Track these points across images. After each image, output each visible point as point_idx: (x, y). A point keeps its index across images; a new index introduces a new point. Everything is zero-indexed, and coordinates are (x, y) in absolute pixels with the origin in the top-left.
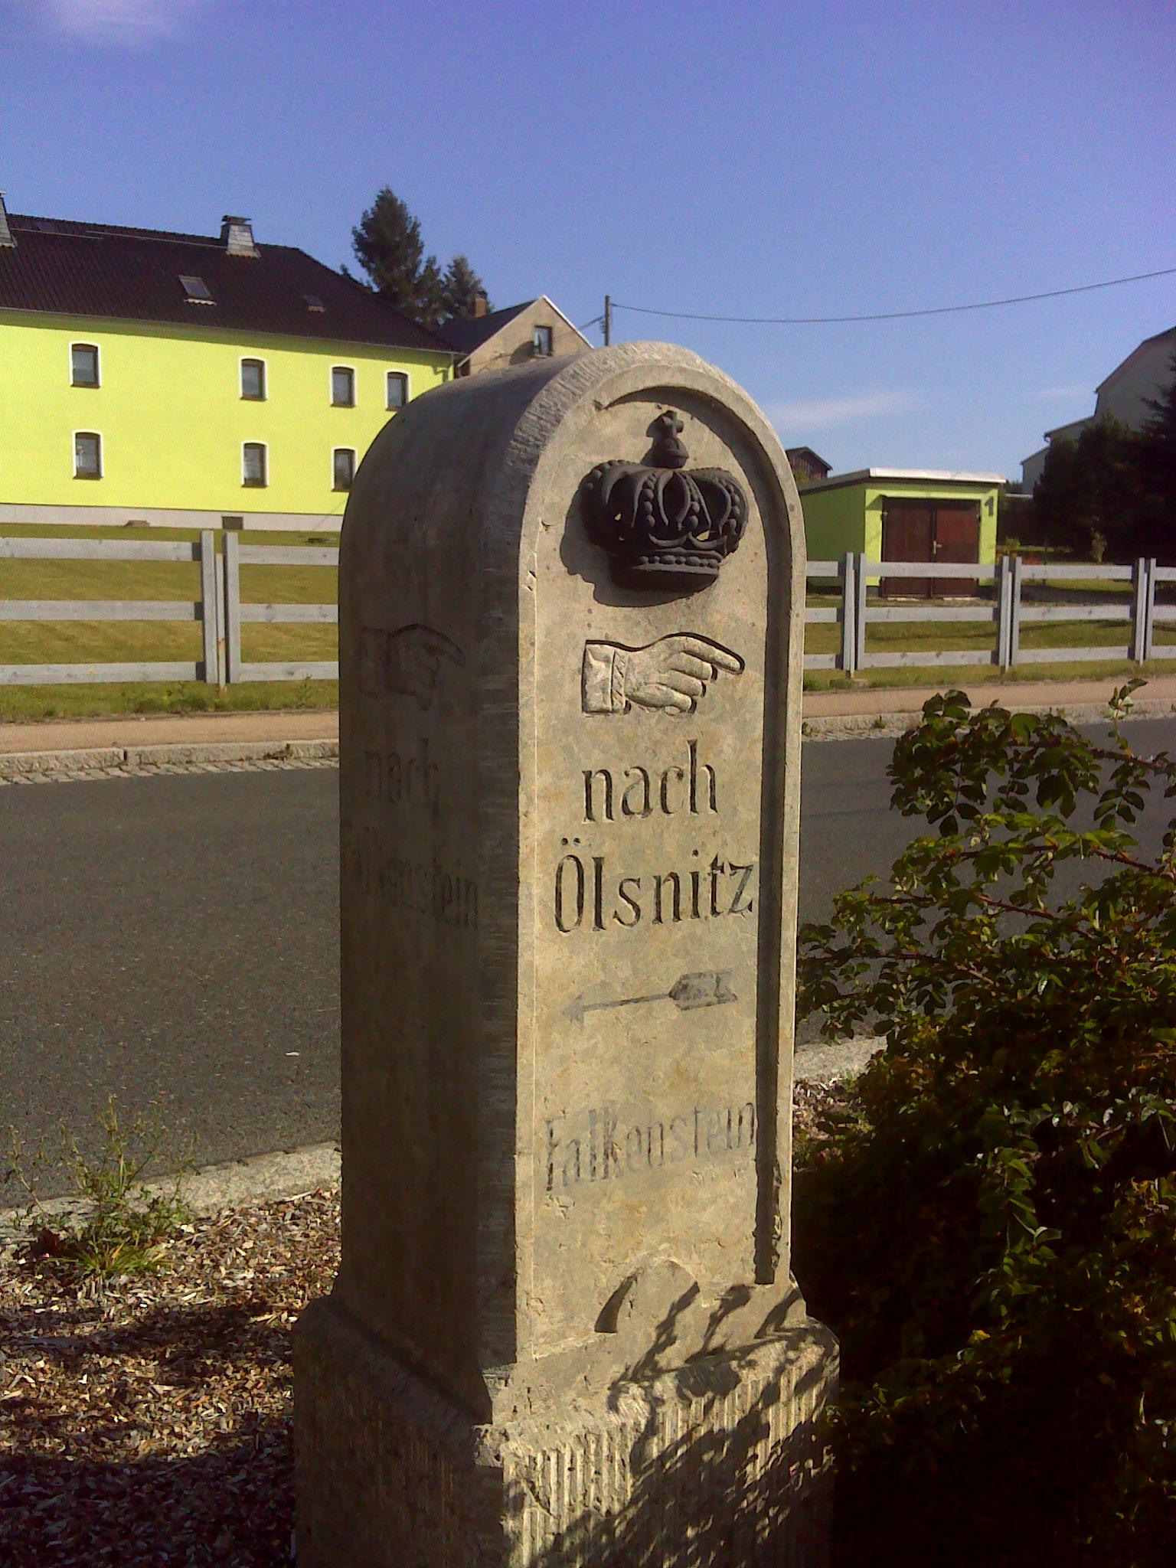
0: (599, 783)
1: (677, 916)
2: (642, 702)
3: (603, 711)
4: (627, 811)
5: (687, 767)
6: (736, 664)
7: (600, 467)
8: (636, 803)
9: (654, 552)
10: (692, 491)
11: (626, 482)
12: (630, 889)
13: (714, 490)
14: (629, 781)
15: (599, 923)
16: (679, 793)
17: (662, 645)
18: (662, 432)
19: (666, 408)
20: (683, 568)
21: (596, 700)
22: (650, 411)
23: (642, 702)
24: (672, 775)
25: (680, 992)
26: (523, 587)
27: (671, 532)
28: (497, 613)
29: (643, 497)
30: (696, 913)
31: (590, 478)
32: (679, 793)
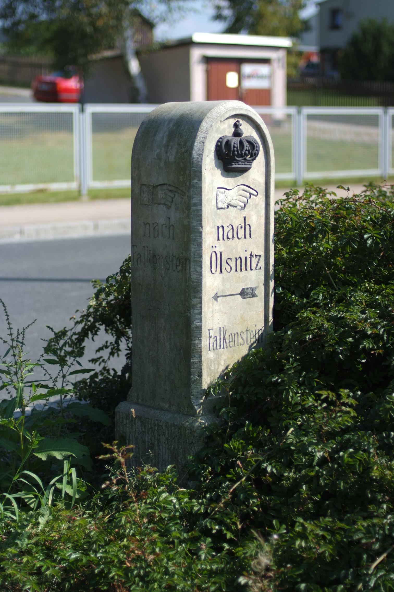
0: (221, 230)
1: (241, 270)
2: (232, 206)
3: (222, 208)
4: (228, 238)
5: (243, 225)
6: (255, 193)
7: (221, 138)
8: (230, 236)
9: (237, 162)
10: (246, 144)
11: (228, 143)
12: (229, 261)
13: (252, 144)
14: (229, 229)
15: (221, 272)
16: (241, 233)
17: (237, 188)
18: (236, 126)
19: (237, 119)
20: (244, 166)
21: (220, 205)
22: (232, 121)
23: (232, 206)
24: (239, 227)
25: (243, 294)
26: (203, 173)
27: (241, 156)
28: (196, 181)
29: (234, 147)
30: (246, 270)
31: (218, 141)
32: (241, 233)
